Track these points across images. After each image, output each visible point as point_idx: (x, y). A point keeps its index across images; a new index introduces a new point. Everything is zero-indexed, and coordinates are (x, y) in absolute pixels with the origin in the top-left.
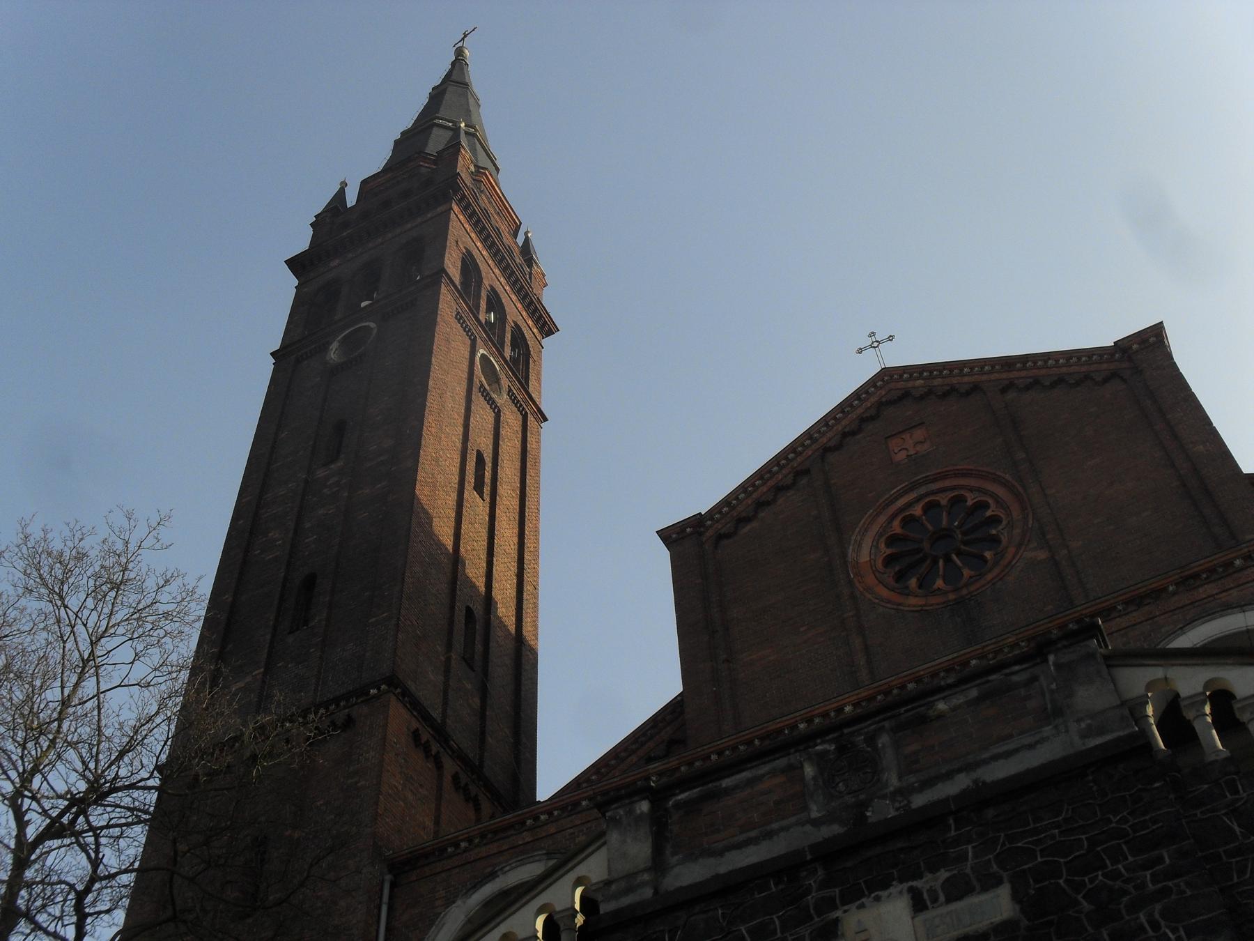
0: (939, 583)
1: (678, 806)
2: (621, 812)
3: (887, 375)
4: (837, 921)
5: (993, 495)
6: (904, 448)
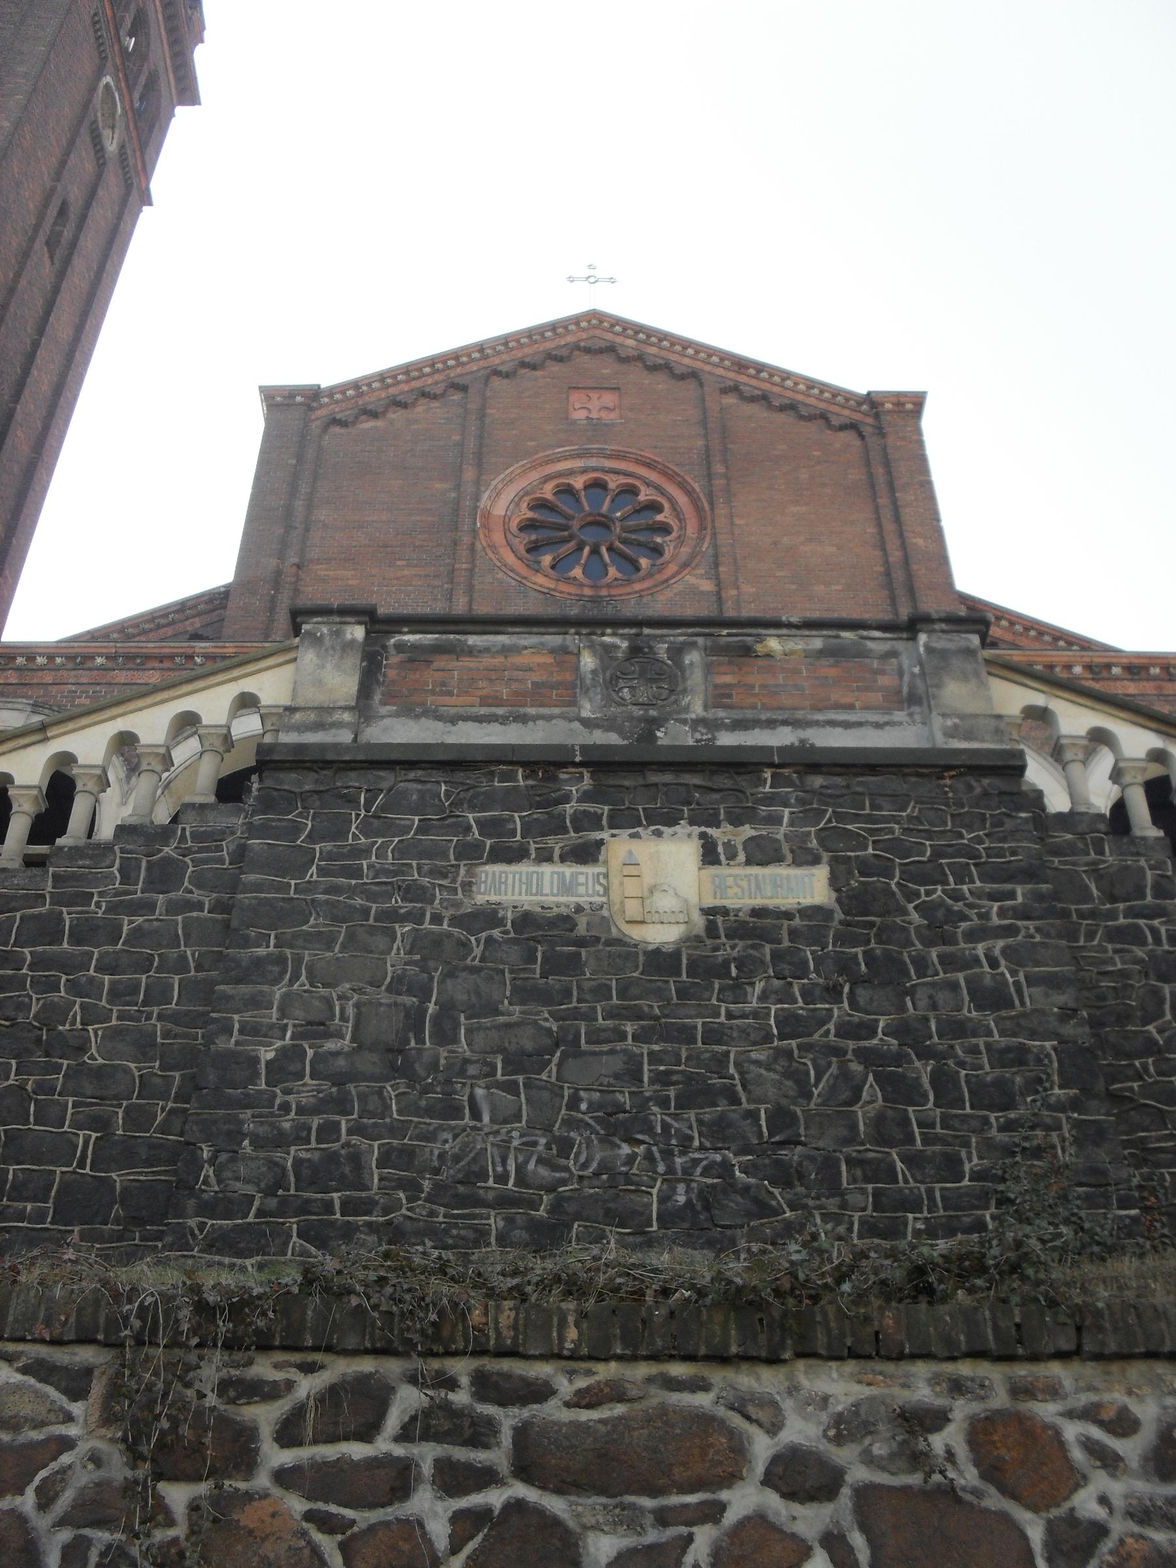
0: (577, 572)
1: (400, 647)
2: (325, 630)
3: (595, 319)
4: (601, 842)
5: (671, 500)
6: (587, 408)
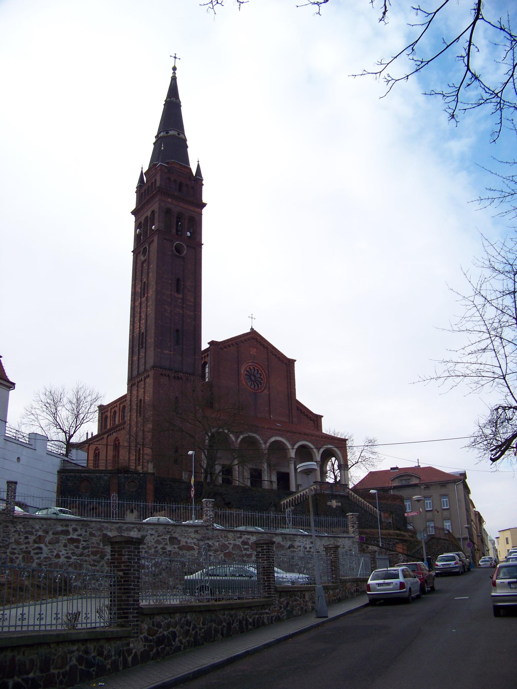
6: (253, 351)
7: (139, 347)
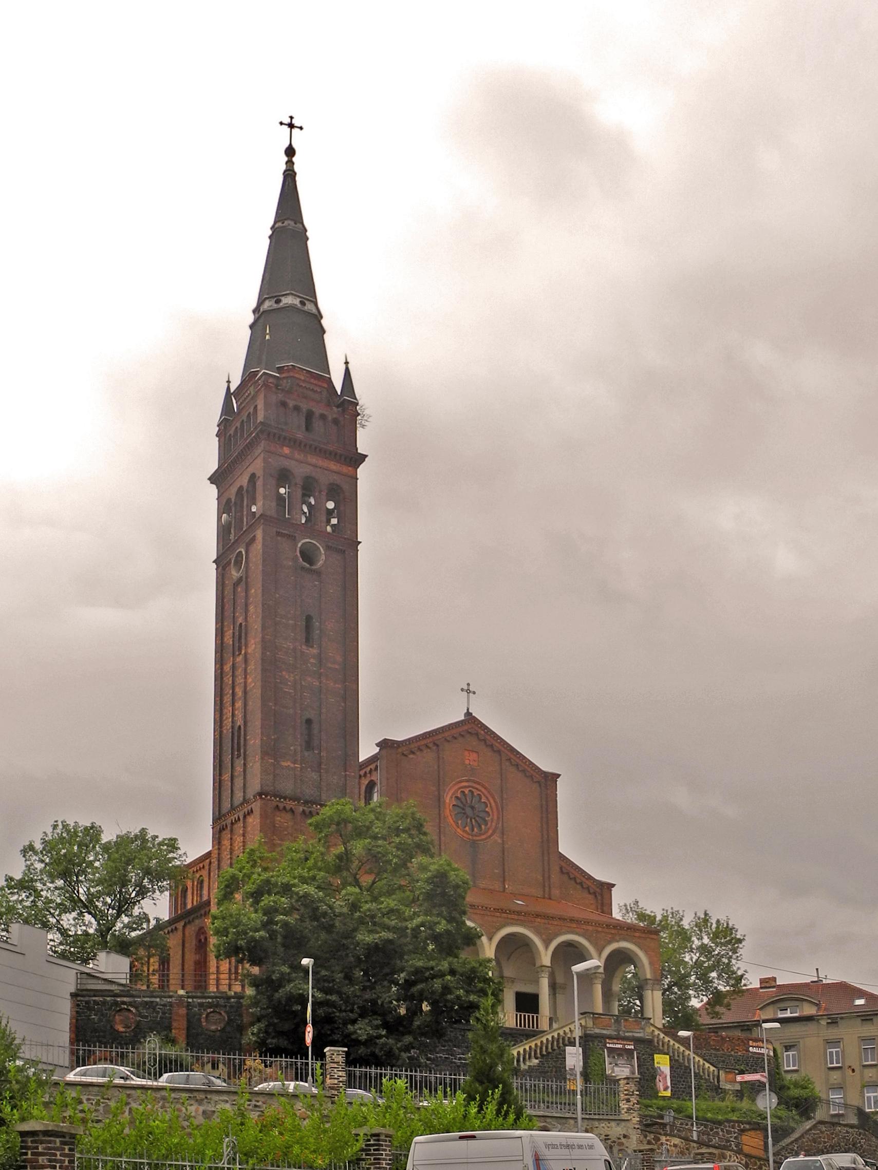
7: (232, 754)
